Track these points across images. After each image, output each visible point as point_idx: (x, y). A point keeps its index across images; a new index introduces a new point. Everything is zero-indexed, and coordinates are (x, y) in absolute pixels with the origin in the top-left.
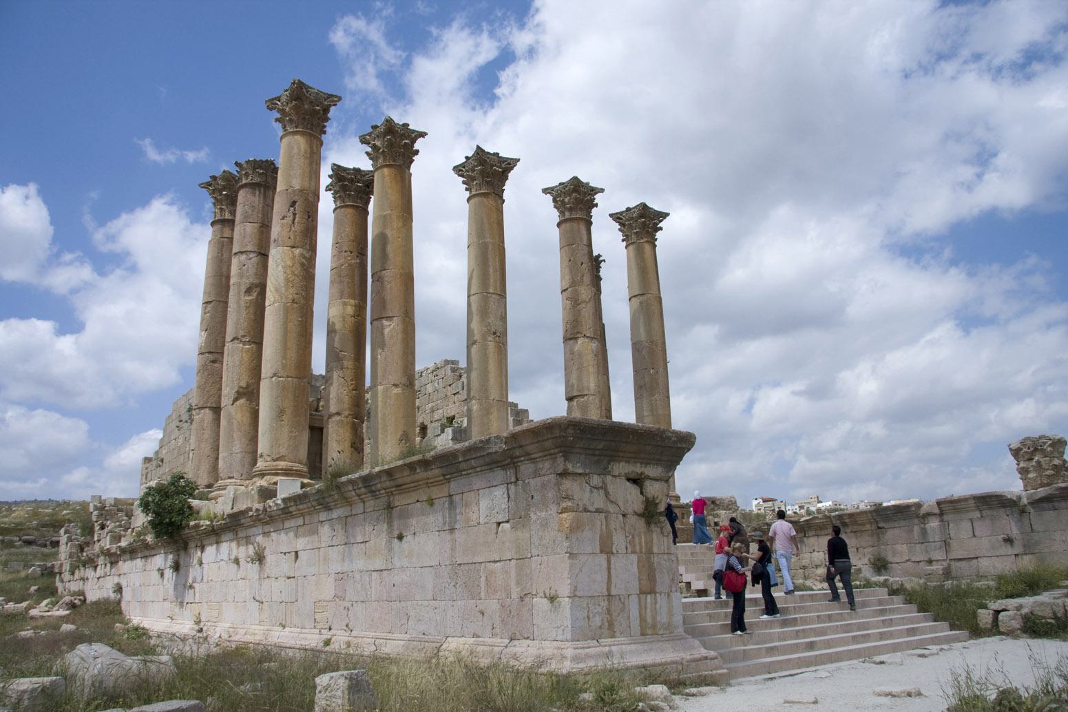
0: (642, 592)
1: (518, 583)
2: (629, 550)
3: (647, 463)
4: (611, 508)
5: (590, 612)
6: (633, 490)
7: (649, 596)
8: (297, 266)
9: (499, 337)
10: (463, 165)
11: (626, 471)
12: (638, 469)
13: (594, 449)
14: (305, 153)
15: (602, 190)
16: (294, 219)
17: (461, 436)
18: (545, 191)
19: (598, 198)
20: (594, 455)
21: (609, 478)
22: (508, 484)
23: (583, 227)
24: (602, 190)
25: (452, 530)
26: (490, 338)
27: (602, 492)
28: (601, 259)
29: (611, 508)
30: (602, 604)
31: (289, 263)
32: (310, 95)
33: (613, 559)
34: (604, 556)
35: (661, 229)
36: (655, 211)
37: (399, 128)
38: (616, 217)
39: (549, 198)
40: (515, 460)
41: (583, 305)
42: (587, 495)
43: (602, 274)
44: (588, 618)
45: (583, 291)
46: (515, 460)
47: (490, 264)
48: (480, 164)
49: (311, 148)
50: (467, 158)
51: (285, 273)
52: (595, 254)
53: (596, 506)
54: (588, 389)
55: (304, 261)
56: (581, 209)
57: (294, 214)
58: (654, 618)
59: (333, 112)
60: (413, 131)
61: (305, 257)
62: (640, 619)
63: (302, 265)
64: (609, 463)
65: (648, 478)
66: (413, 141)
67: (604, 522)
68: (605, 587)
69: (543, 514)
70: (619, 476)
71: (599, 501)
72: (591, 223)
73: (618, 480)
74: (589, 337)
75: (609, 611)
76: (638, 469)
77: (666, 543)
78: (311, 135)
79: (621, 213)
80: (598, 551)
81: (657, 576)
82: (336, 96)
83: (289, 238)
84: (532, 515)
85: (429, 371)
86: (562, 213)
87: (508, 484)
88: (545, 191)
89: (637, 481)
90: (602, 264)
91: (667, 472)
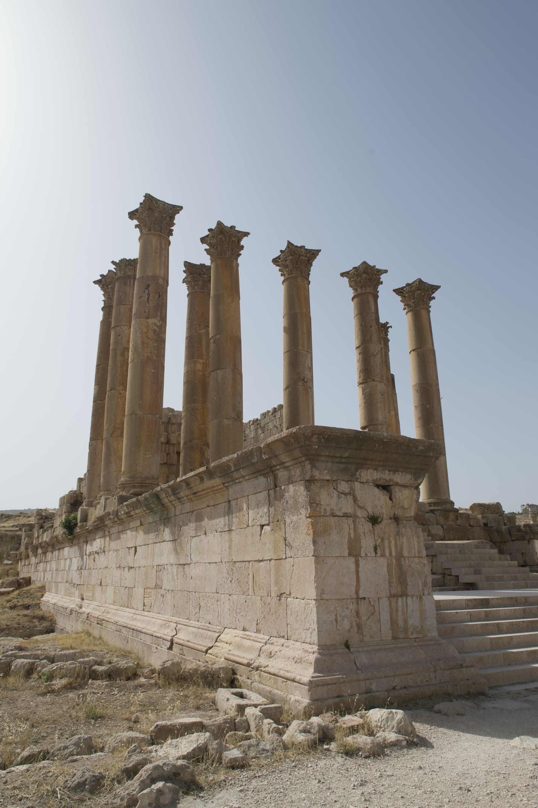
0: (392, 596)
1: (276, 583)
2: (379, 554)
5: (338, 615)
6: (381, 497)
7: (400, 600)
10: (279, 257)
11: (375, 478)
12: (386, 476)
13: (342, 457)
16: (148, 298)
18: (342, 275)
19: (383, 277)
20: (342, 463)
21: (357, 485)
22: (269, 490)
23: (371, 299)
24: (386, 271)
25: (230, 530)
27: (350, 499)
28: (388, 325)
29: (359, 513)
30: (351, 607)
31: (145, 330)
32: (159, 206)
33: (362, 562)
34: (353, 559)
35: (434, 298)
38: (398, 291)
39: (346, 280)
40: (274, 469)
42: (334, 500)
43: (389, 337)
44: (336, 621)
46: (274, 469)
48: (291, 255)
49: (161, 245)
50: (281, 251)
51: (142, 337)
52: (382, 320)
53: (344, 510)
55: (156, 328)
57: (149, 295)
58: (406, 621)
59: (178, 218)
60: (239, 232)
62: (391, 622)
63: (155, 331)
64: (357, 470)
65: (397, 484)
66: (239, 241)
67: (352, 526)
68: (354, 590)
69: (295, 518)
70: (367, 482)
71: (347, 506)
72: (378, 296)
73: (366, 485)
75: (358, 614)
76: (386, 476)
77: (416, 544)
78: (160, 236)
79: (402, 288)
80: (347, 555)
81: (408, 579)
82: (179, 206)
83: (145, 312)
84: (287, 519)
85: (270, 414)
86: (355, 290)
87: (269, 490)
88: (342, 275)
89: (385, 488)
90: (390, 330)
91: (416, 479)
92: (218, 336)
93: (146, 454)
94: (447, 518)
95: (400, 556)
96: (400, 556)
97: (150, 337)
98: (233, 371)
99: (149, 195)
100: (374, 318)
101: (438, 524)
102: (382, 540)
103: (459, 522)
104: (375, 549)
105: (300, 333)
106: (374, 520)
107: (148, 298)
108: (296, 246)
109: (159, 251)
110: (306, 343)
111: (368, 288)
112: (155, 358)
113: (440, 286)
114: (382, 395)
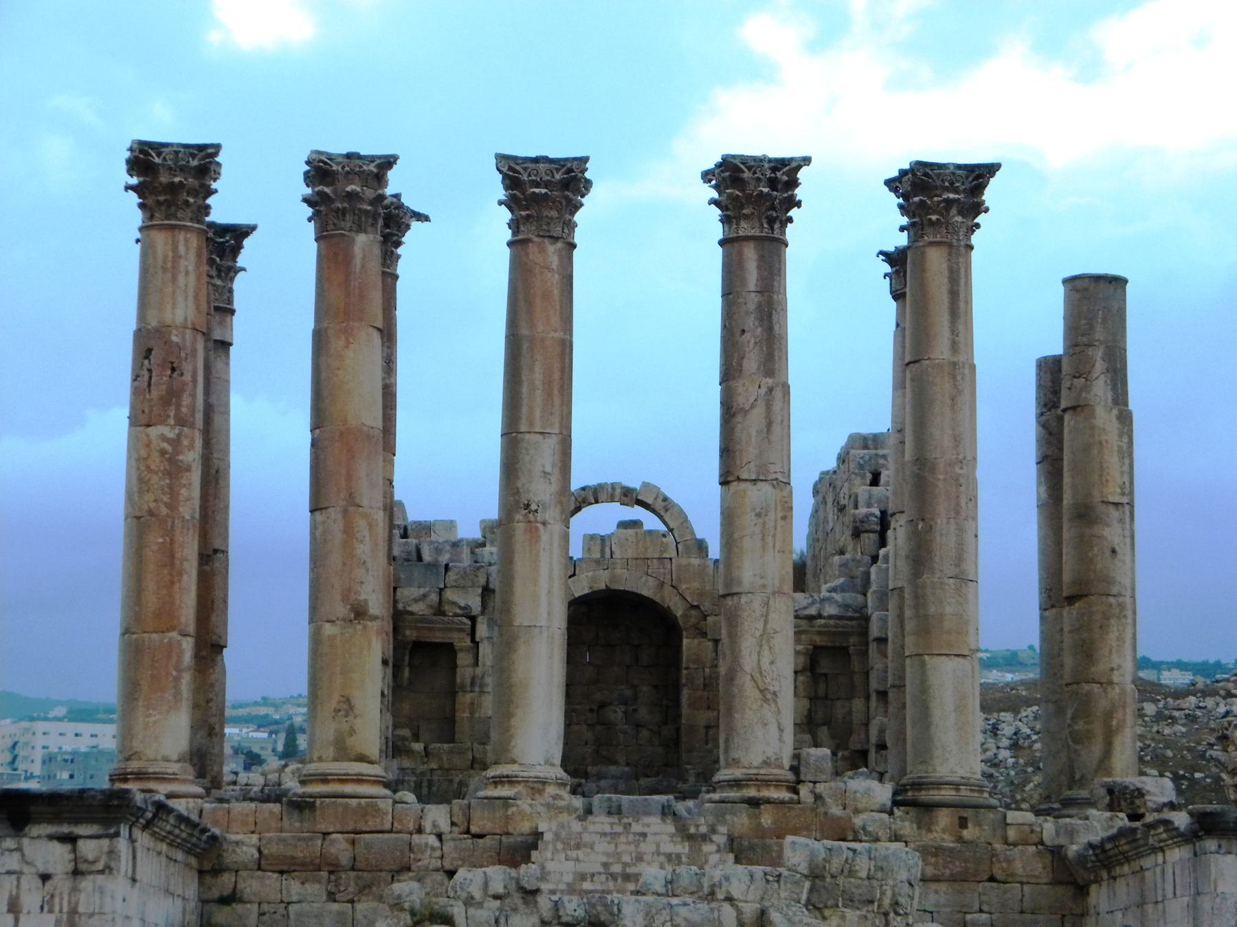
3: (77, 821)
4: (26, 869)
8: (155, 455)
9: (536, 511)
12: (65, 829)
14: (165, 262)
15: (807, 161)
16: (150, 378)
21: (25, 841)
23: (750, 253)
24: (807, 161)
26: (519, 517)
27: (16, 855)
32: (165, 159)
33: (22, 918)
36: (959, 167)
37: (338, 164)
41: (739, 418)
45: (740, 390)
47: (524, 378)
51: (138, 469)
54: (740, 583)
55: (165, 445)
56: (746, 217)
57: (150, 371)
60: (371, 159)
67: (15, 883)
74: (746, 480)
76: (65, 829)
78: (173, 227)
89: (71, 840)
92: (317, 431)
93: (150, 715)
94: (924, 825)
95: (73, 912)
96: (73, 912)
97: (153, 467)
98: (345, 512)
100: (752, 307)
102: (52, 896)
103: (966, 834)
104: (42, 908)
105: (525, 390)
106: (45, 878)
107: (150, 378)
108: (526, 159)
109: (169, 265)
111: (743, 224)
112: (164, 511)
114: (759, 515)
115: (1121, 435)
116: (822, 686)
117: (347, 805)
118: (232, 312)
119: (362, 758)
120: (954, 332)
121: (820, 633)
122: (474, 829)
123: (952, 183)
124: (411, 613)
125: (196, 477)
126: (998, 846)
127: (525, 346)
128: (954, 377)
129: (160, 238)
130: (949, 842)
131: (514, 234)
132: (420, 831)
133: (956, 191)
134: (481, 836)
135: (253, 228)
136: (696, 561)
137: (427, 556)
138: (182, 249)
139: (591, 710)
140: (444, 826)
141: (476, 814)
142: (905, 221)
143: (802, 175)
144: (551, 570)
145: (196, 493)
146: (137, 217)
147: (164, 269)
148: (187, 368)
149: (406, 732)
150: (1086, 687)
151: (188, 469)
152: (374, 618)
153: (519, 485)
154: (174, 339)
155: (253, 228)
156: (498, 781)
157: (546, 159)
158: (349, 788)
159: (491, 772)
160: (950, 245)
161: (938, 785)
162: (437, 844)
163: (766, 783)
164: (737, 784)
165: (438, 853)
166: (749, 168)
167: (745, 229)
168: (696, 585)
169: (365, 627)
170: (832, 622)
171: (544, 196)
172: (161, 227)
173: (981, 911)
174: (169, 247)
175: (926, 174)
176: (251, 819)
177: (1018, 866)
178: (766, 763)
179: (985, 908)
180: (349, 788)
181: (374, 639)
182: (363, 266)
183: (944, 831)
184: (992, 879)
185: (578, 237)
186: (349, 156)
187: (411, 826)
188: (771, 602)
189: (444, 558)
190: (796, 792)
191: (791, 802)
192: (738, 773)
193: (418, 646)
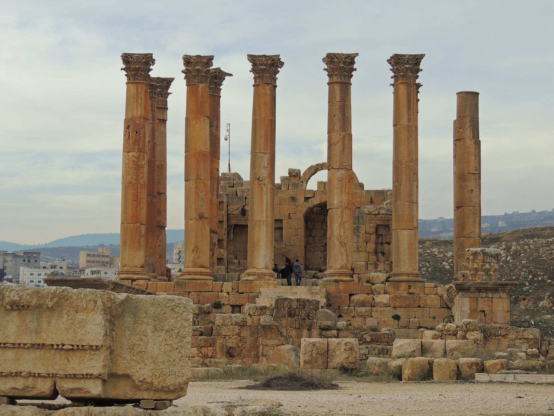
8: (131, 162)
14: (134, 95)
15: (357, 54)
17: (358, 221)
23: (337, 88)
24: (357, 54)
26: (256, 182)
31: (127, 162)
36: (410, 55)
41: (333, 147)
45: (334, 136)
49: (137, 91)
56: (336, 75)
61: (135, 157)
63: (133, 161)
94: (397, 288)
98: (196, 181)
99: (125, 54)
100: (337, 107)
101: (385, 293)
105: (258, 138)
108: (258, 56)
110: (262, 146)
111: (335, 77)
112: (134, 182)
113: (424, 55)
114: (340, 181)
115: (475, 149)
116: (380, 239)
117: (196, 283)
118: (167, 109)
119: (202, 267)
120: (409, 115)
121: (379, 220)
122: (240, 291)
123: (408, 62)
124: (233, 214)
125: (146, 170)
126: (422, 295)
127: (258, 122)
128: (409, 131)
129: (132, 87)
130: (405, 294)
131: (255, 82)
132: (222, 291)
133: (409, 64)
134: (243, 293)
135: (174, 79)
136: (359, 191)
137: (239, 194)
138: (140, 91)
139: (322, 246)
140: (230, 290)
141: (241, 286)
142: (393, 74)
143: (356, 59)
144: (267, 201)
145: (146, 175)
146: (125, 79)
147: (134, 98)
148: (142, 132)
149: (233, 256)
150: (462, 239)
151: (143, 167)
152: (206, 218)
153: (256, 171)
154: (137, 122)
155: (174, 79)
156: (249, 275)
157: (265, 56)
158: (197, 277)
159: (247, 271)
160: (408, 83)
161: (401, 274)
162: (228, 296)
163: (341, 274)
164: (332, 275)
165: (228, 299)
166: (337, 58)
167: (335, 79)
168: (359, 200)
169: (203, 221)
170: (383, 216)
171: (266, 69)
172: (132, 83)
173: (415, 318)
174: (135, 90)
175: (398, 59)
176: (164, 287)
177: (429, 302)
178: (341, 268)
179: (417, 316)
180: (197, 277)
181: (206, 225)
182: (202, 95)
183: (403, 290)
184: (419, 306)
185: (278, 83)
186: (197, 56)
187: (219, 290)
188: (344, 212)
189: (245, 195)
190: (353, 277)
191: (350, 281)
192: (332, 271)
193: (236, 226)
